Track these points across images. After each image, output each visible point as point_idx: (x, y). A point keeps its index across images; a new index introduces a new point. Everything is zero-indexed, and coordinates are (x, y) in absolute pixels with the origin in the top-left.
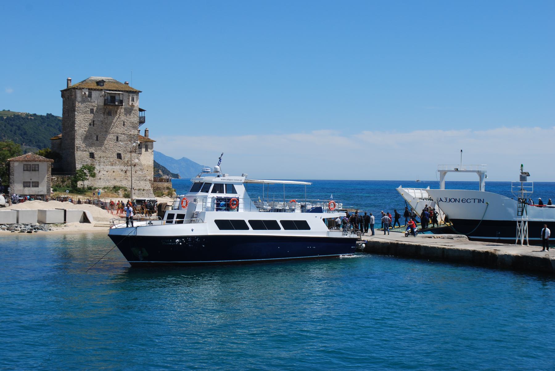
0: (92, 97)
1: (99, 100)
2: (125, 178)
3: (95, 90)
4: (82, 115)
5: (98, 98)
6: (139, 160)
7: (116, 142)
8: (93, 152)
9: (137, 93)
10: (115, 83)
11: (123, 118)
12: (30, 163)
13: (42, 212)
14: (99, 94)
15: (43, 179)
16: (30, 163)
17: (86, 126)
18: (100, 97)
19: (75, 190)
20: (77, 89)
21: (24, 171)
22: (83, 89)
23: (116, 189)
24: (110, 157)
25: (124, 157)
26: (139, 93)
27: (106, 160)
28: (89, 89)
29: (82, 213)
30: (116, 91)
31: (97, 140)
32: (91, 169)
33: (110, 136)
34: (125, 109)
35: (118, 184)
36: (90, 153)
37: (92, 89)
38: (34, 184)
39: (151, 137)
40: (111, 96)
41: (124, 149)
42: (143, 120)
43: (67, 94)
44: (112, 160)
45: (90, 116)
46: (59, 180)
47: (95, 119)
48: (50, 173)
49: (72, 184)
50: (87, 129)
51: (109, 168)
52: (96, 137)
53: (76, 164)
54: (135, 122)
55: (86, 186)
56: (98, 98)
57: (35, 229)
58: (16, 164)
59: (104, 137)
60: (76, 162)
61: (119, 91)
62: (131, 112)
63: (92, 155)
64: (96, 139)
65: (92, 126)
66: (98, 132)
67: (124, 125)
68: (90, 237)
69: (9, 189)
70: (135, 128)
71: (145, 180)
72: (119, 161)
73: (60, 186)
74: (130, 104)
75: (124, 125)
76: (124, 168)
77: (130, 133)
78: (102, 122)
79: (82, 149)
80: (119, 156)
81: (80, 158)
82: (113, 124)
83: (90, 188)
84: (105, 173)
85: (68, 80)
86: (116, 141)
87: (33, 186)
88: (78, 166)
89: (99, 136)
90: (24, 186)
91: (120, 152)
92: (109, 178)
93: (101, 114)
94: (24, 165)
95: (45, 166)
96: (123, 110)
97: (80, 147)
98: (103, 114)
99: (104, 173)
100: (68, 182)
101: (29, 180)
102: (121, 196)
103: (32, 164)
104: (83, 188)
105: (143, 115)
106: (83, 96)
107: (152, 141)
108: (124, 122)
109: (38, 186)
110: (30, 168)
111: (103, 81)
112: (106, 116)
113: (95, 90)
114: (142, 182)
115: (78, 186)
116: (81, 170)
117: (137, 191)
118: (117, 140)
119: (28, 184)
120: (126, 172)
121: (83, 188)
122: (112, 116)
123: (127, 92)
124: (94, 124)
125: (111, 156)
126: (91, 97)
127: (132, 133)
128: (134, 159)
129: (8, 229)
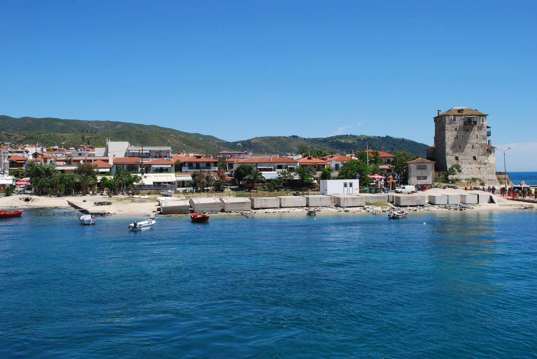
0: (456, 120)
2: (479, 172)
3: (458, 115)
4: (450, 133)
8: (458, 156)
9: (485, 116)
10: (470, 110)
11: (476, 133)
12: (421, 164)
13: (463, 197)
14: (461, 118)
15: (429, 174)
16: (421, 164)
19: (446, 180)
20: (446, 115)
21: (417, 169)
22: (450, 115)
23: (474, 180)
24: (468, 159)
25: (478, 159)
26: (487, 116)
28: (454, 115)
29: (489, 196)
30: (471, 115)
31: (460, 148)
32: (458, 167)
33: (469, 145)
34: (478, 127)
35: (475, 177)
36: (456, 157)
37: (456, 115)
38: (423, 178)
39: (493, 144)
40: (468, 119)
42: (489, 134)
43: (438, 120)
44: (470, 161)
45: (455, 133)
46: (437, 175)
48: (434, 171)
49: (445, 177)
50: (453, 141)
51: (468, 166)
53: (447, 164)
55: (454, 178)
57: (463, 208)
58: (412, 165)
60: (447, 163)
61: (473, 115)
62: (481, 129)
63: (457, 158)
65: (456, 139)
67: (477, 137)
68: (495, 213)
69: (408, 181)
70: (485, 139)
71: (493, 174)
72: (475, 162)
73: (437, 179)
74: (481, 123)
75: (477, 137)
76: (478, 166)
77: (481, 142)
78: (463, 136)
79: (450, 154)
80: (475, 158)
82: (470, 138)
83: (457, 180)
84: (466, 169)
85: (438, 110)
87: (423, 179)
88: (449, 166)
89: (461, 146)
90: (418, 179)
91: (475, 156)
92: (469, 173)
94: (417, 165)
95: (430, 166)
96: (476, 128)
97: (449, 153)
100: (442, 176)
101: (421, 175)
102: (478, 184)
104: (453, 180)
105: (489, 131)
106: (450, 120)
107: (494, 148)
109: (426, 179)
110: (421, 167)
111: (462, 110)
112: (465, 132)
113: (458, 115)
114: (490, 175)
115: (449, 178)
116: (452, 168)
117: (487, 181)
118: (473, 148)
119: (420, 178)
120: (479, 169)
121: (453, 180)
123: (479, 115)
127: (483, 142)
129: (445, 208)
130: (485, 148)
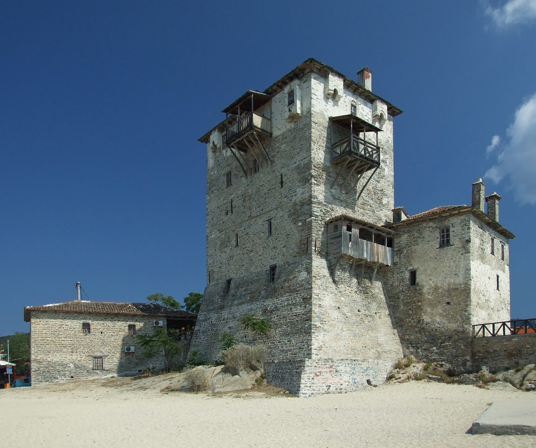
6: (309, 273)
25: (280, 273)
41: (284, 250)
91: (275, 263)
93: (242, 177)
99: (232, 325)
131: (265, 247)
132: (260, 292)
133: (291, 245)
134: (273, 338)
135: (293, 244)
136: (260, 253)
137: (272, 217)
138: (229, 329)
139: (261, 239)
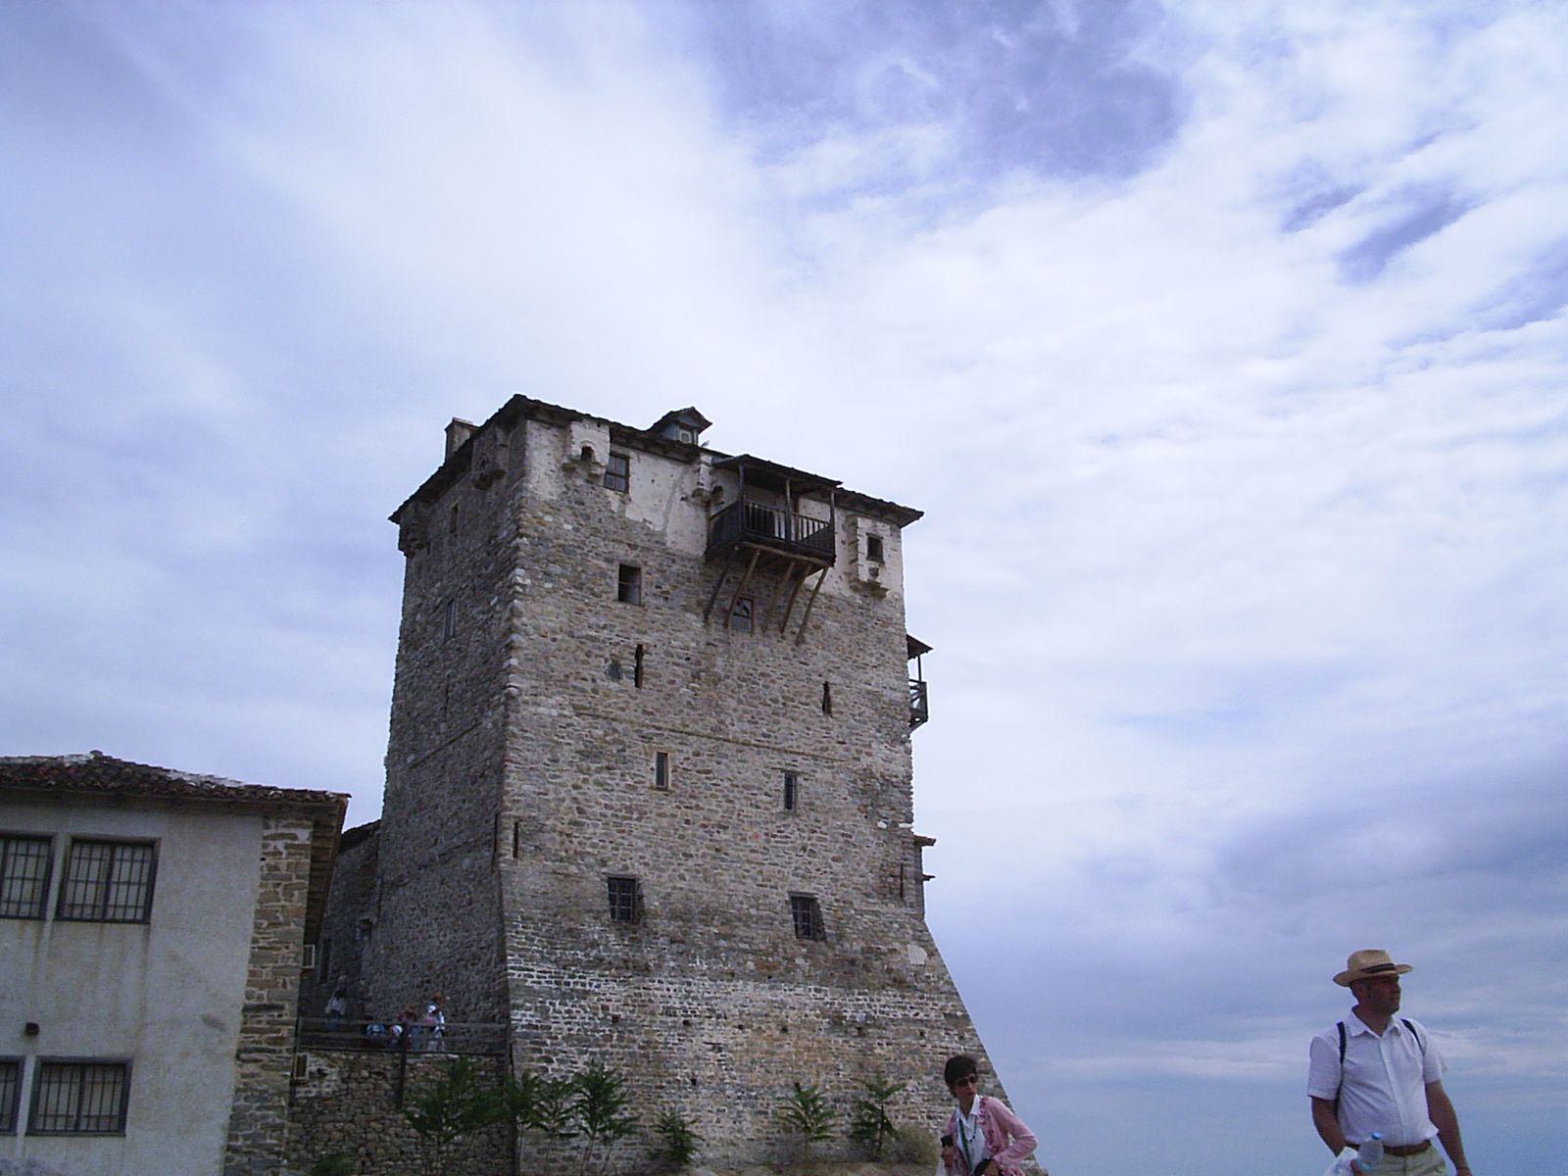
1: (670, 517)
5: (669, 508)
7: (784, 815)
8: (637, 870)
17: (585, 674)
18: (682, 499)
27: (726, 937)
41: (837, 867)
47: (645, 639)
51: (750, 994)
52: (654, 765)
54: (889, 693)
56: (670, 502)
59: (709, 772)
64: (654, 778)
66: (666, 733)
67: (827, 706)
75: (827, 706)
77: (865, 761)
81: (537, 914)
86: (781, 807)
91: (807, 888)
93: (686, 609)
98: (700, 610)
103: (77, 841)
108: (826, 686)
112: (716, 633)
122: (758, 630)
124: (638, 670)
125: (753, 911)
126: (626, 491)
128: (897, 945)
130: (895, 824)
131: (775, 836)
132: (791, 960)
133: (859, 864)
134: (905, 1103)
135: (863, 865)
136: (753, 844)
137: (798, 770)
138: (709, 1050)
139: (758, 807)
